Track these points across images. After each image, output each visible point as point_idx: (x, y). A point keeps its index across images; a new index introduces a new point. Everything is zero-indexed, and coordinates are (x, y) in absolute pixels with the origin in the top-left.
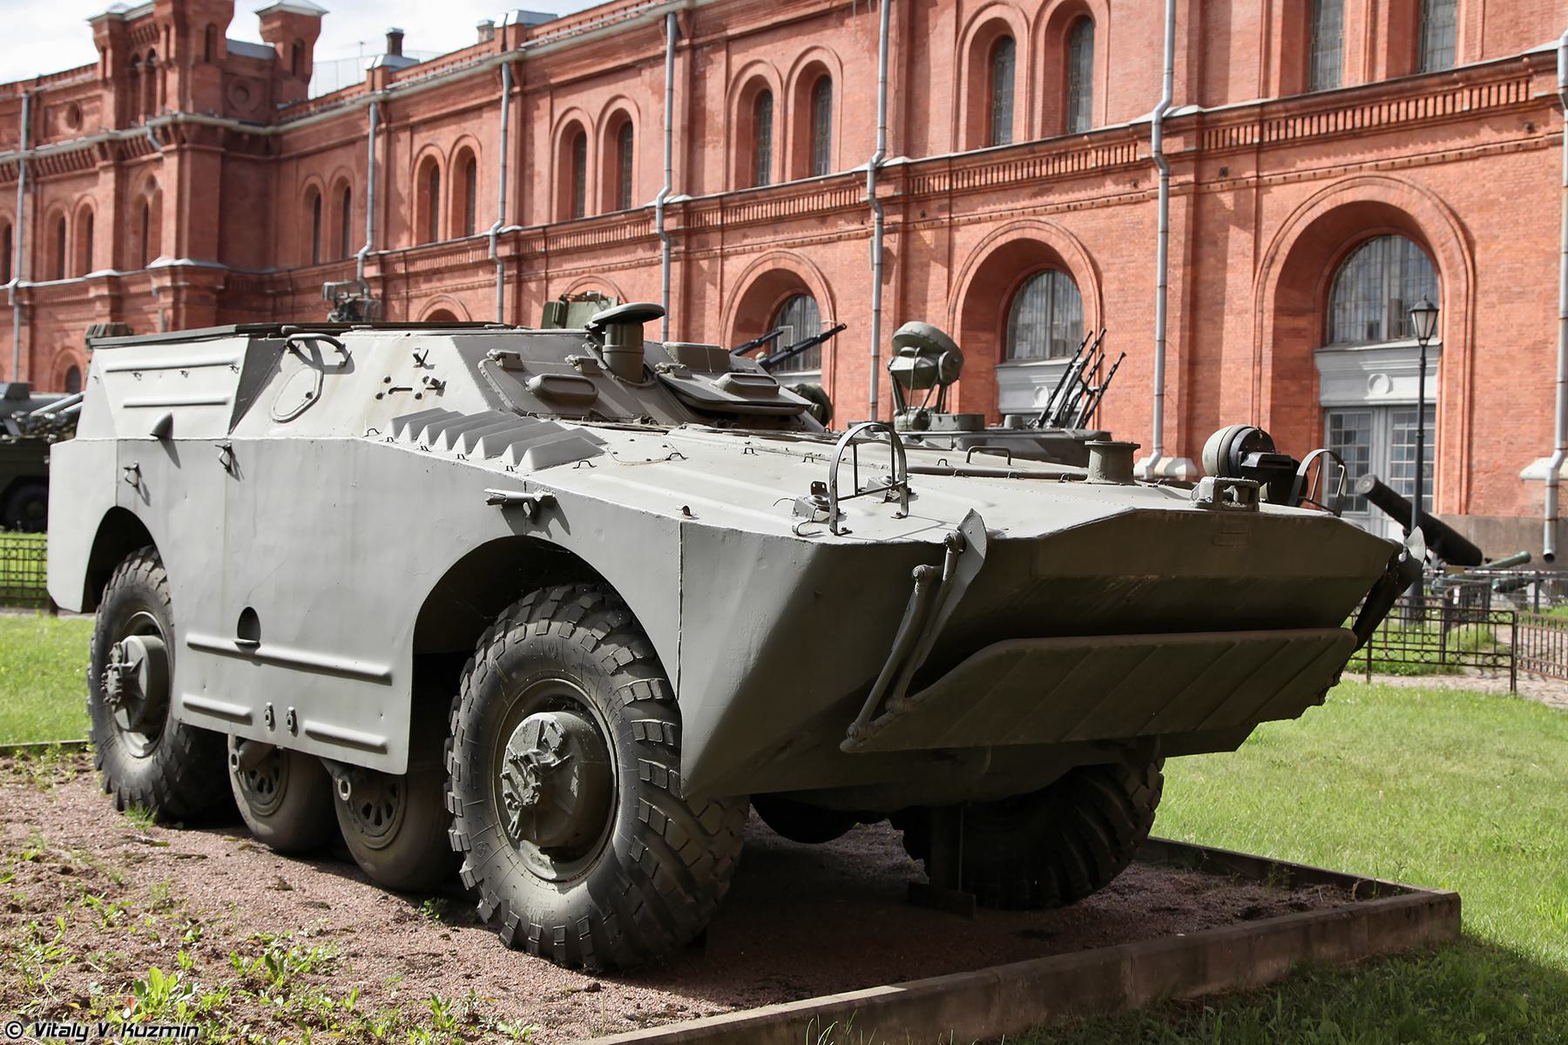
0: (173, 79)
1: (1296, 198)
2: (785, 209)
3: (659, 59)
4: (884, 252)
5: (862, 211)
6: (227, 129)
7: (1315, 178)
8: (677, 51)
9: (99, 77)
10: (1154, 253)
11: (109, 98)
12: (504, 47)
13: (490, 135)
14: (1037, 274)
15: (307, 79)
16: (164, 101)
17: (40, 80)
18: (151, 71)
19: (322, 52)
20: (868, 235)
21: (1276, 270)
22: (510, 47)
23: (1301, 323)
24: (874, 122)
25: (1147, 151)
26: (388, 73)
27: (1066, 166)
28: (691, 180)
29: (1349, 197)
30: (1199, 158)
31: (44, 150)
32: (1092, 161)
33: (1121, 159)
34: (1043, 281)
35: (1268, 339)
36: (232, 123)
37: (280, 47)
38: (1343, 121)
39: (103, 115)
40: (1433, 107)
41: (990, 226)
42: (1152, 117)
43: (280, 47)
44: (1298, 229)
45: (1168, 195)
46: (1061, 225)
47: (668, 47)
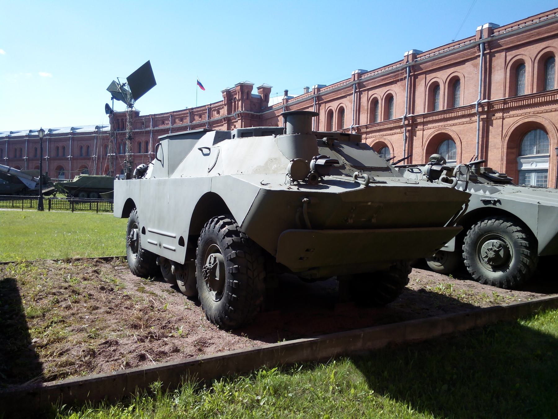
0: (240, 103)
1: (514, 120)
2: (382, 127)
3: (352, 94)
4: (406, 137)
5: (401, 127)
6: (251, 114)
7: (517, 116)
8: (356, 92)
10: (476, 135)
11: (226, 108)
14: (445, 141)
15: (268, 102)
16: (238, 108)
17: (211, 105)
18: (235, 102)
19: (271, 95)
20: (402, 133)
21: (507, 138)
23: (514, 151)
24: (404, 107)
25: (474, 111)
26: (287, 100)
27: (453, 115)
28: (358, 121)
29: (527, 120)
30: (487, 113)
31: (212, 119)
32: (460, 114)
33: (467, 113)
34: (446, 142)
35: (505, 154)
36: (252, 113)
38: (525, 102)
39: (224, 112)
40: (549, 99)
41: (433, 130)
42: (476, 103)
43: (262, 95)
44: (513, 128)
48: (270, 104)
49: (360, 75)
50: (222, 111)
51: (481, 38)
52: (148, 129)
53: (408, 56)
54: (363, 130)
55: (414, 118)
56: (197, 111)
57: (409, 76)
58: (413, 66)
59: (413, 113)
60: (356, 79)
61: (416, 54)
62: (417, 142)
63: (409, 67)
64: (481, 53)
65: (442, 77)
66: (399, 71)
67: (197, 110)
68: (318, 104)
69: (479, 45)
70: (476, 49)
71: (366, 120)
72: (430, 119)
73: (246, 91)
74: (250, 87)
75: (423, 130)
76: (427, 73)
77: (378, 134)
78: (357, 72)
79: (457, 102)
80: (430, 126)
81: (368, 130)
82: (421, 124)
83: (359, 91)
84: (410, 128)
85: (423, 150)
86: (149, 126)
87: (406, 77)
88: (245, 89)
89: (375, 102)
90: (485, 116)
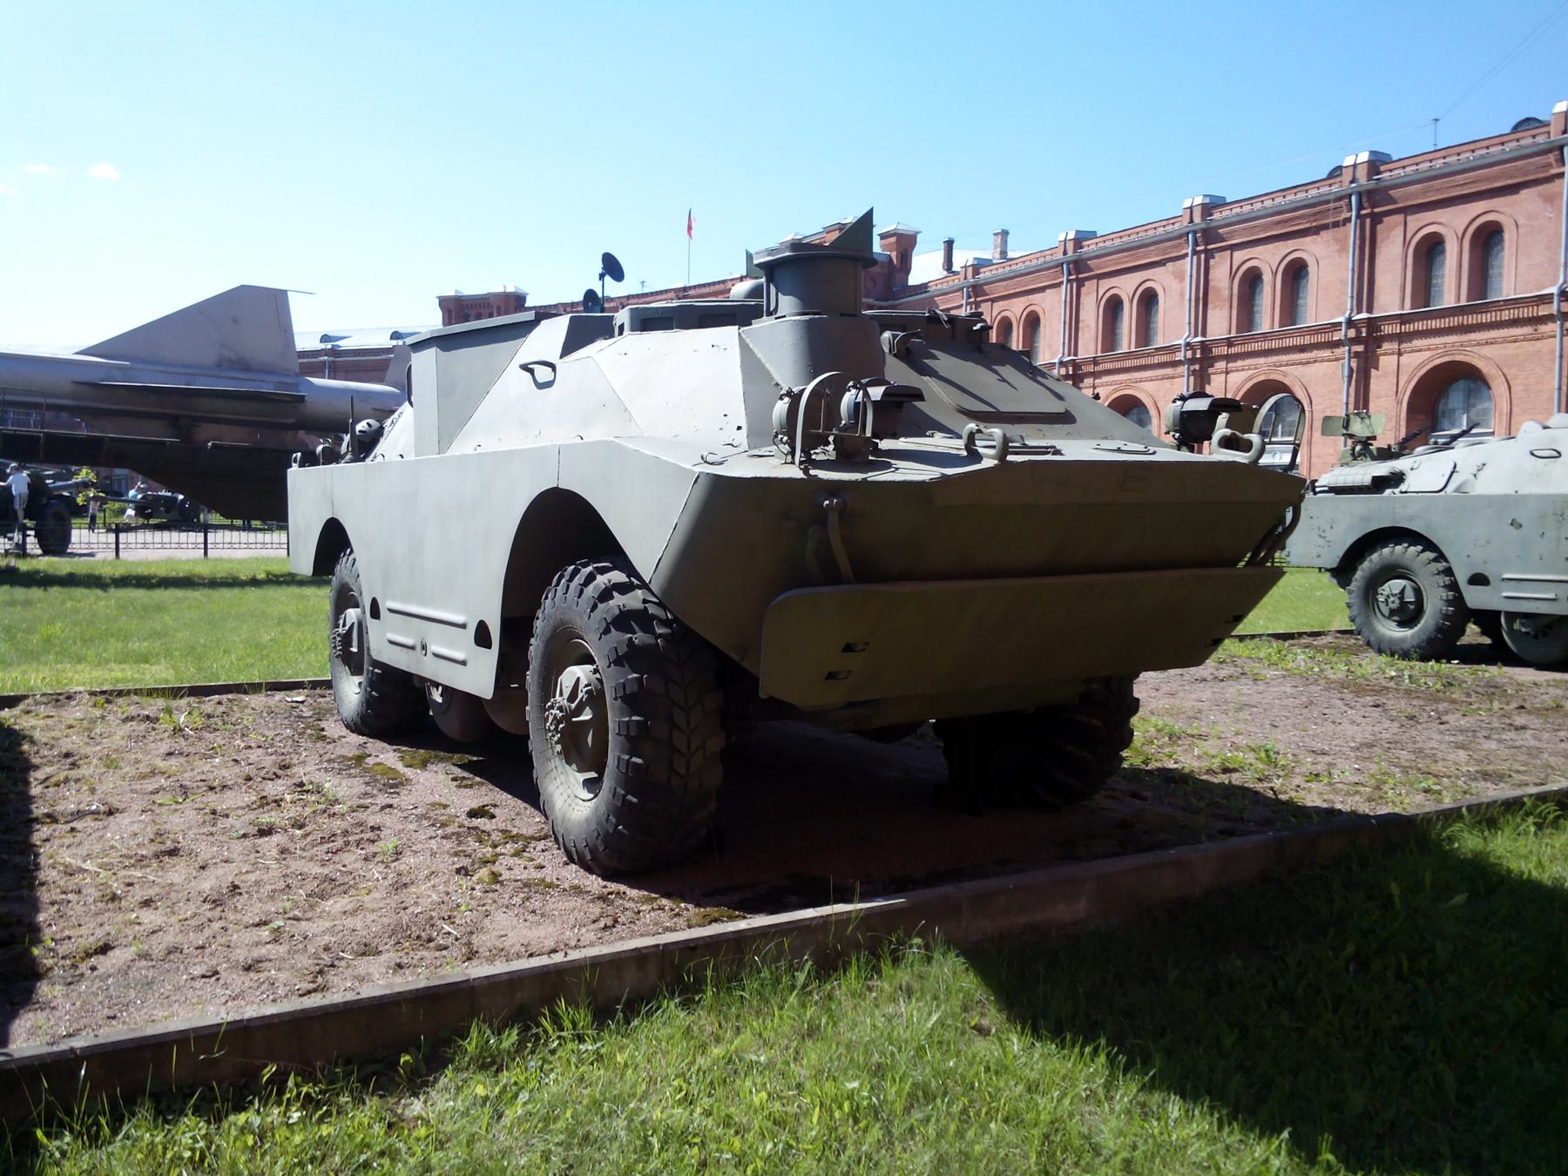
4: (1351, 370)
8: (1195, 252)
10: (1551, 369)
12: (1065, 253)
15: (908, 271)
20: (1337, 360)
22: (1070, 253)
28: (1201, 325)
32: (1506, 315)
33: (1528, 315)
34: (1461, 384)
37: (894, 255)
41: (1429, 354)
43: (894, 255)
45: (1562, 336)
46: (1482, 351)
47: (1189, 250)
48: (914, 279)
49: (1208, 209)
53: (1355, 166)
54: (1216, 351)
55: (1373, 324)
57: (1358, 216)
58: (1370, 192)
59: (1370, 310)
60: (1197, 219)
61: (1377, 163)
62: (1381, 383)
63: (1360, 195)
65: (1454, 224)
66: (1328, 202)
68: (1077, 280)
70: (1552, 158)
71: (1225, 324)
75: (1400, 354)
76: (1407, 211)
77: (1262, 360)
78: (1199, 200)
79: (1493, 283)
80: (1417, 343)
81: (1233, 350)
83: (1206, 251)
84: (1360, 348)
85: (1400, 403)
87: (1348, 220)
89: (1252, 280)
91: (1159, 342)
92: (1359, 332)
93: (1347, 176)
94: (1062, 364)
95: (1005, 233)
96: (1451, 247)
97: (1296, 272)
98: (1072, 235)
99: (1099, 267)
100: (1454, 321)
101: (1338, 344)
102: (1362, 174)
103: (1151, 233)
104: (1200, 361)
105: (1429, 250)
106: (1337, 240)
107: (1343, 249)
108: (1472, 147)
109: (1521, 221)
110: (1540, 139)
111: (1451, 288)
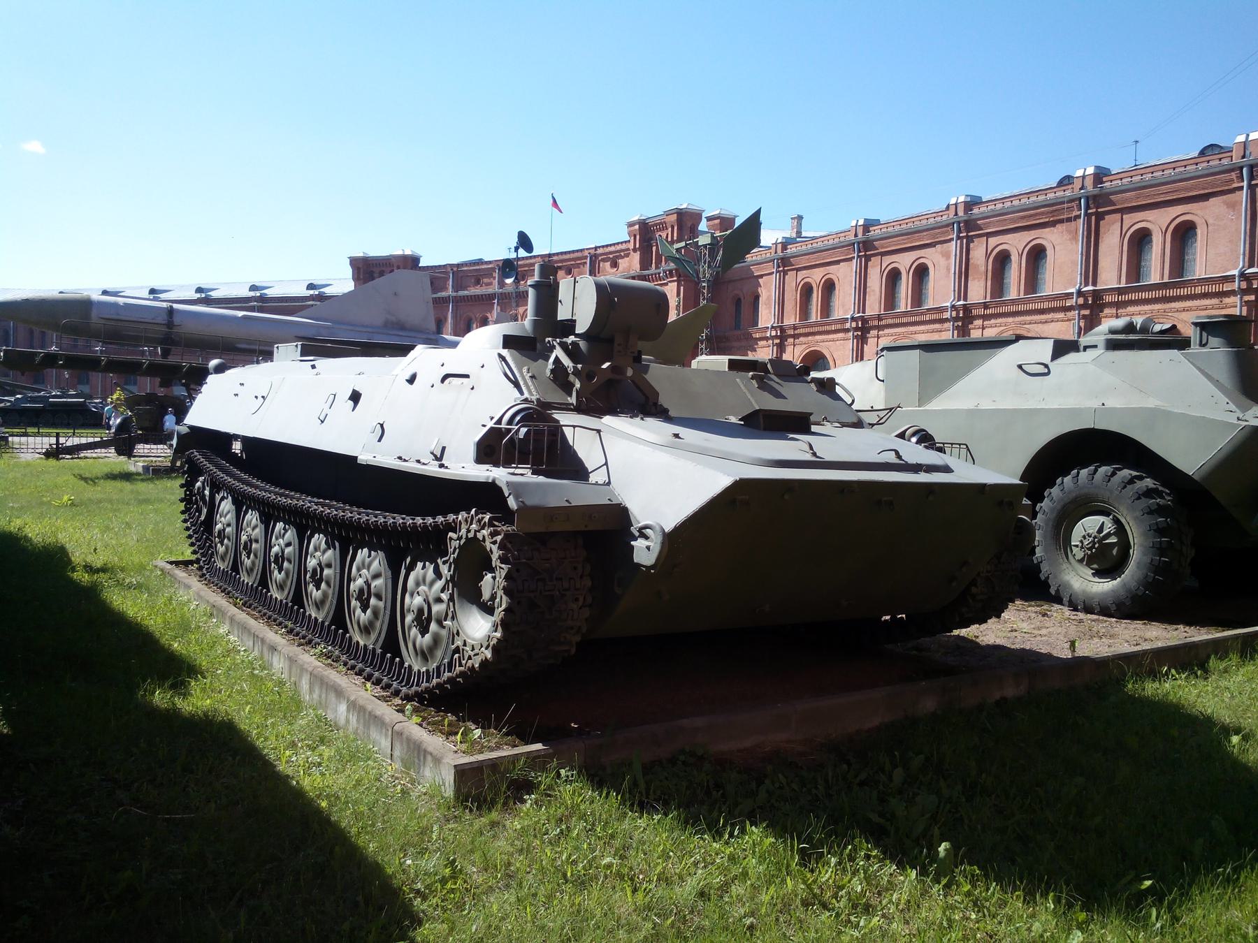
8: (959, 238)
9: (631, 246)
11: (636, 257)
13: (845, 275)
17: (596, 248)
20: (1069, 320)
22: (860, 236)
28: (963, 292)
32: (1198, 290)
42: (1236, 272)
50: (623, 263)
51: (1244, 157)
52: (443, 294)
53: (1084, 177)
54: (975, 312)
55: (1097, 294)
56: (562, 261)
57: (1086, 214)
58: (1095, 197)
60: (961, 213)
63: (1087, 198)
64: (1245, 184)
65: (1159, 222)
66: (1063, 203)
67: (561, 257)
69: (1241, 168)
70: (1234, 175)
71: (982, 292)
72: (1133, 296)
73: (689, 224)
74: (696, 216)
76: (1123, 211)
77: (1010, 320)
78: (962, 199)
81: (989, 312)
82: (1111, 305)
84: (1087, 312)
86: (445, 288)
87: (1079, 217)
88: (686, 221)
89: (1003, 259)
90: (1253, 298)
91: (930, 303)
92: (1086, 300)
93: (1078, 184)
94: (853, 319)
95: (800, 218)
96: (1157, 240)
97: (1037, 255)
98: (861, 222)
99: (882, 246)
100: (1159, 294)
101: (1070, 308)
102: (1089, 183)
103: (924, 222)
104: (962, 319)
105: (1140, 240)
106: (1069, 232)
107: (1075, 238)
108: (1173, 165)
109: (1210, 221)
110: (1225, 162)
111: (1156, 268)
